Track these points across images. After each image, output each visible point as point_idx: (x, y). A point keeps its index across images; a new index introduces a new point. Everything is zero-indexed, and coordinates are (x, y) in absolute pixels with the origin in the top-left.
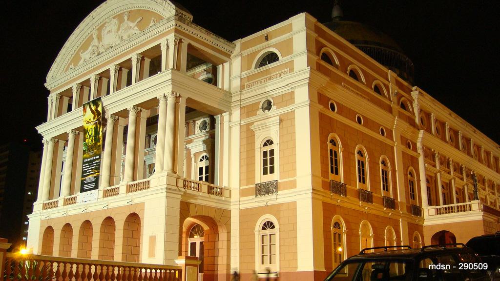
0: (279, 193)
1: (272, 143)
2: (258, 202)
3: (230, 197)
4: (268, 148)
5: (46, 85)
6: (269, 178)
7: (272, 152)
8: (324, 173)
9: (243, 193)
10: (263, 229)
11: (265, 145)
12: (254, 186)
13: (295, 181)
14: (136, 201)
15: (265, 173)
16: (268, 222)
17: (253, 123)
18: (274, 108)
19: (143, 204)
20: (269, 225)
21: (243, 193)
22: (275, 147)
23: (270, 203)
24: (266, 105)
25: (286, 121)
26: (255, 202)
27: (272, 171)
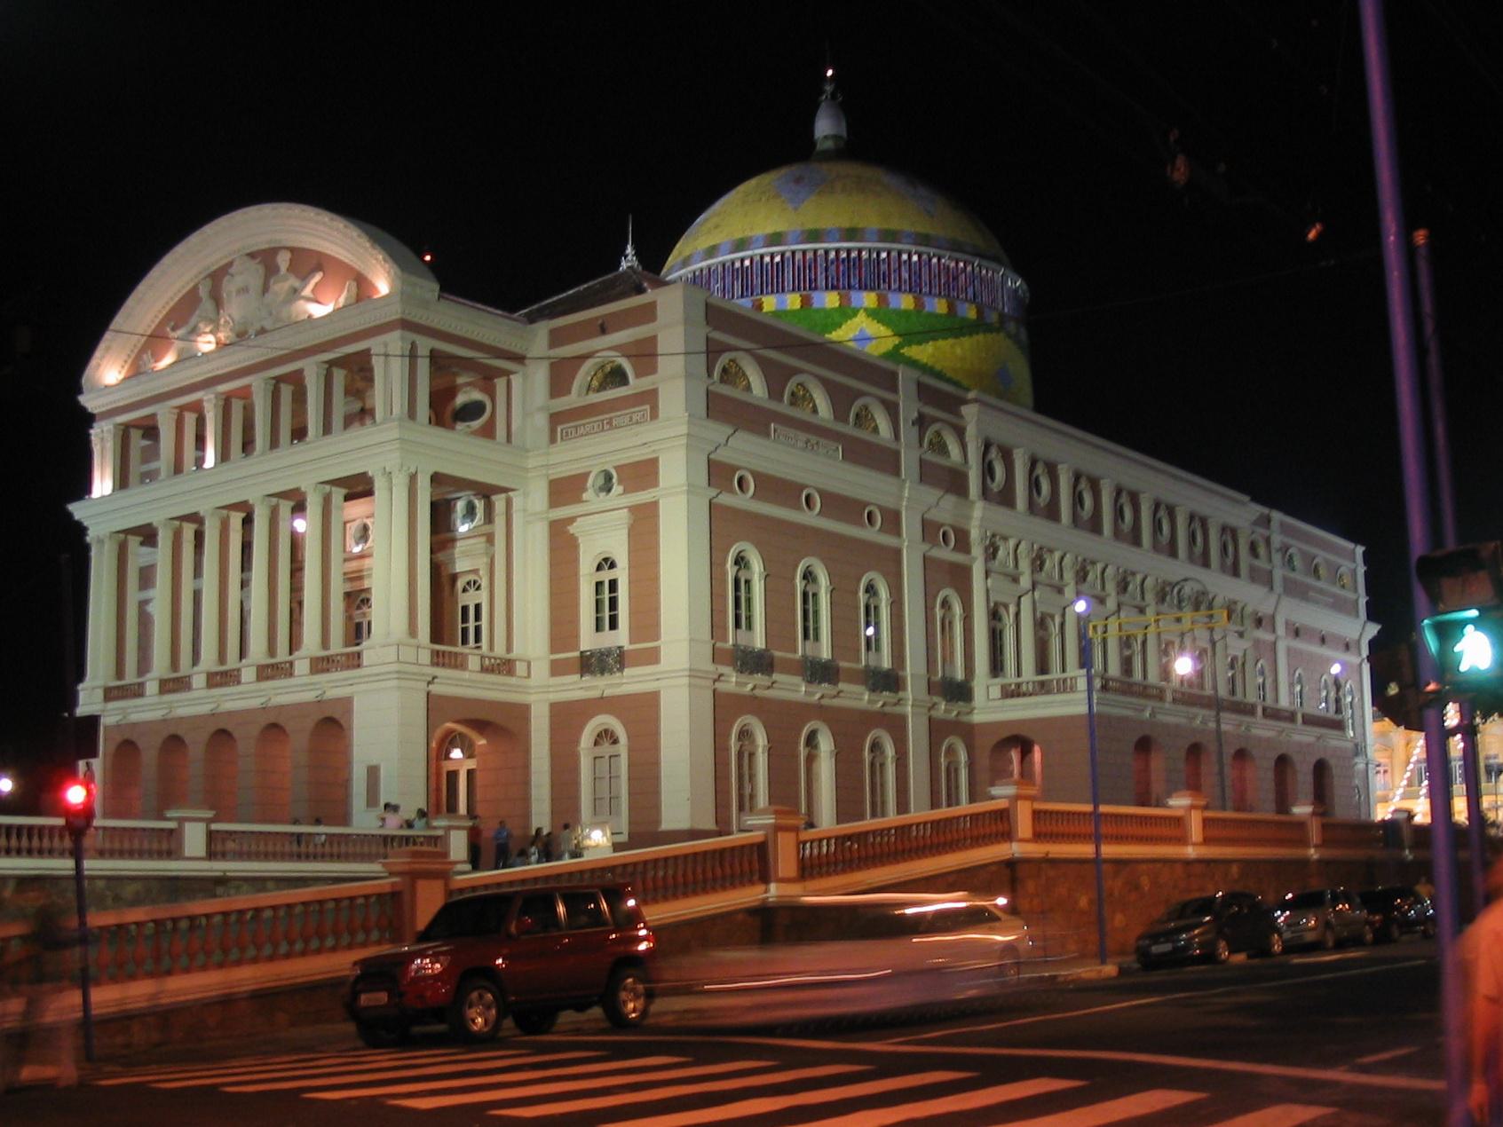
0: (626, 671)
1: (612, 566)
2: (586, 689)
3: (529, 676)
4: (606, 576)
5: (82, 399)
6: (609, 640)
7: (613, 585)
8: (717, 629)
9: (557, 669)
10: (596, 743)
11: (599, 568)
12: (577, 654)
13: (656, 650)
14: (333, 693)
15: (599, 628)
16: (606, 731)
17: (572, 520)
18: (617, 489)
19: (347, 703)
20: (606, 736)
21: (557, 669)
22: (622, 574)
23: (608, 693)
24: (601, 481)
25: (644, 524)
26: (578, 688)
27: (613, 625)
